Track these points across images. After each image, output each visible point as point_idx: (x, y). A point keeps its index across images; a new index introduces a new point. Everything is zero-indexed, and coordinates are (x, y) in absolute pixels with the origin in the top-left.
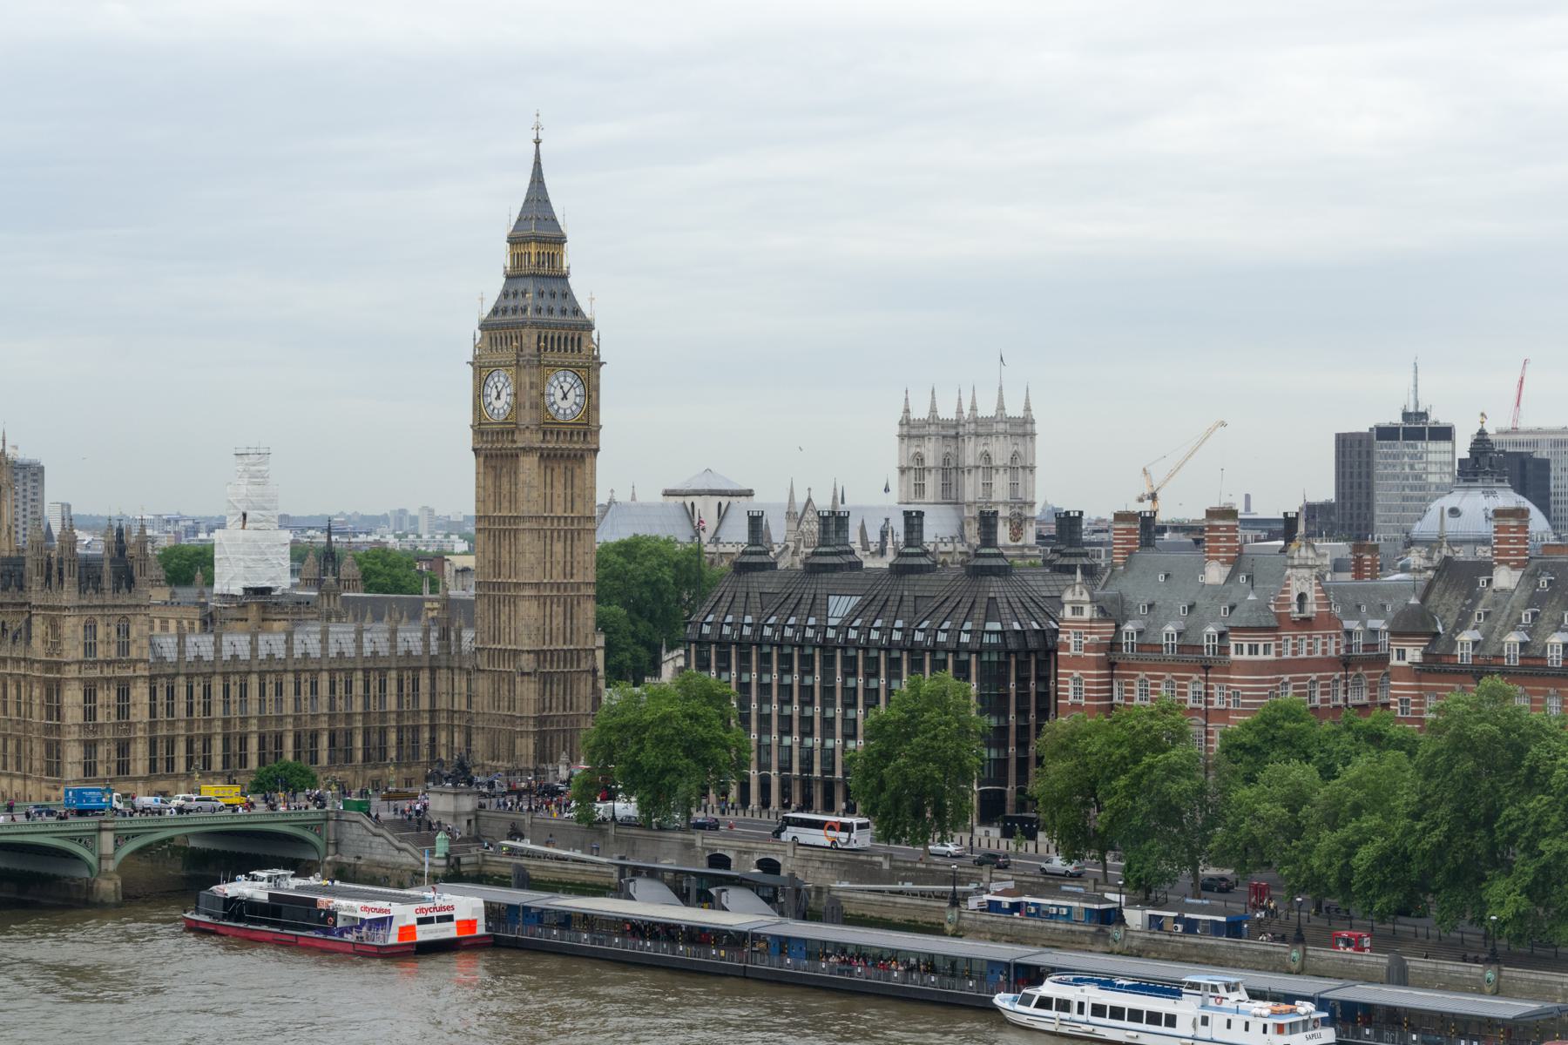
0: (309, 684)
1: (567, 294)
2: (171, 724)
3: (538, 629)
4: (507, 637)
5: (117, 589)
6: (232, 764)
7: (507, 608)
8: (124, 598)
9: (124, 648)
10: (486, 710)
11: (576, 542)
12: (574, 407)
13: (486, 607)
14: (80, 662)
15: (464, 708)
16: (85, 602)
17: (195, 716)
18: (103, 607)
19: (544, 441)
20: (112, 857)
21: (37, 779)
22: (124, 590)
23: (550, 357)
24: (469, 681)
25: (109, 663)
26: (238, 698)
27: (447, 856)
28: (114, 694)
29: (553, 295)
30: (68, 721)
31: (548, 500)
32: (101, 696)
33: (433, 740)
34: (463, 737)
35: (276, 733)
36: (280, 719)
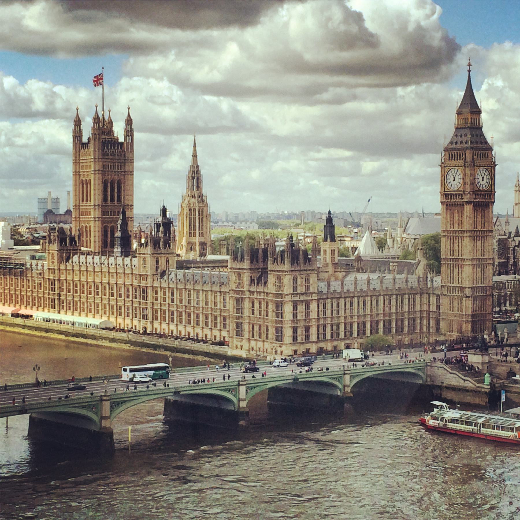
1: (482, 135)
2: (325, 319)
7: (457, 269)
9: (308, 288)
12: (486, 184)
14: (292, 294)
15: (435, 310)
16: (293, 269)
18: (300, 271)
19: (475, 199)
20: (348, 386)
25: (302, 294)
27: (491, 384)
28: (304, 307)
31: (475, 224)
32: (299, 307)
33: (420, 323)
35: (363, 322)
36: (365, 316)
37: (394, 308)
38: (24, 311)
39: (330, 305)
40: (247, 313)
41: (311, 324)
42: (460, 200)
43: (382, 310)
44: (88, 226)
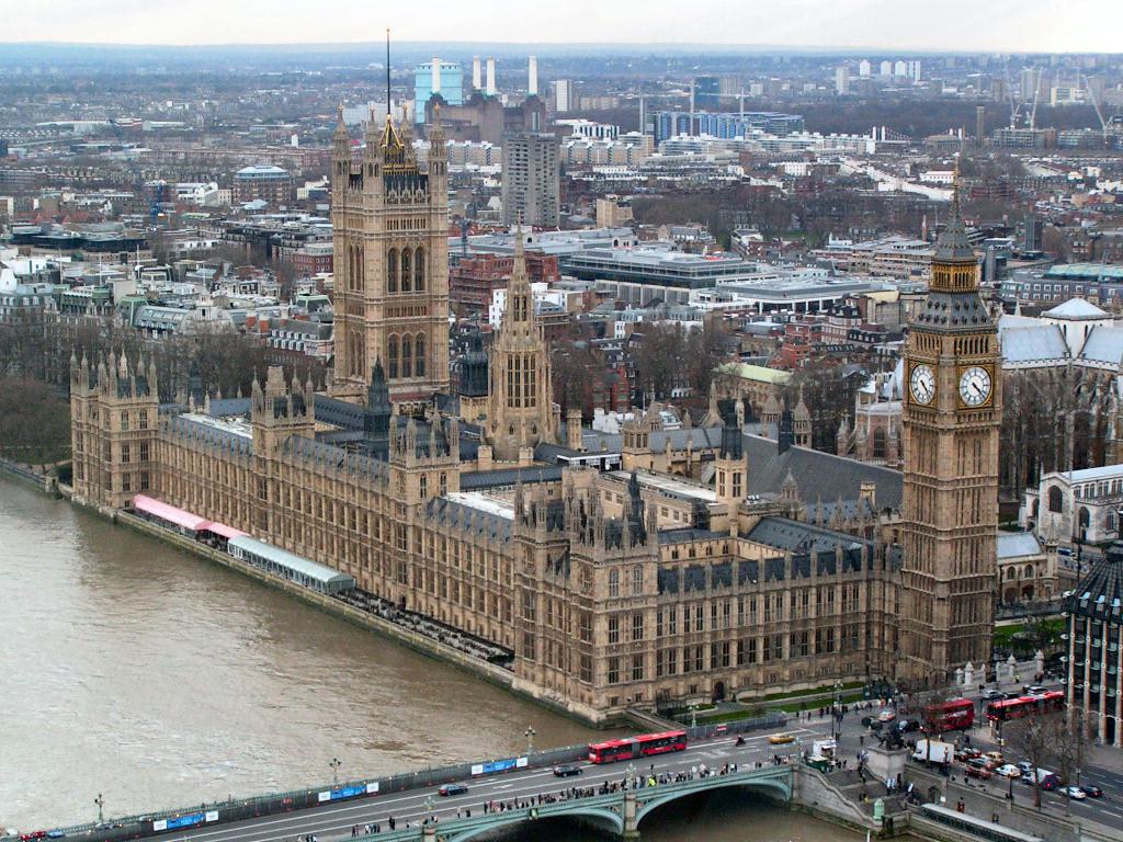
2: (673, 639)
3: (951, 565)
5: (633, 544)
8: (639, 550)
9: (638, 585)
11: (982, 495)
15: (892, 612)
16: (610, 556)
17: (691, 631)
18: (623, 559)
19: (959, 423)
22: (639, 544)
23: (964, 359)
24: (897, 598)
27: (883, 818)
28: (631, 621)
29: (966, 307)
30: (598, 645)
31: (961, 467)
33: (868, 632)
34: (891, 632)
38: (219, 528)
40: (540, 622)
41: (644, 651)
42: (932, 425)
43: (788, 615)
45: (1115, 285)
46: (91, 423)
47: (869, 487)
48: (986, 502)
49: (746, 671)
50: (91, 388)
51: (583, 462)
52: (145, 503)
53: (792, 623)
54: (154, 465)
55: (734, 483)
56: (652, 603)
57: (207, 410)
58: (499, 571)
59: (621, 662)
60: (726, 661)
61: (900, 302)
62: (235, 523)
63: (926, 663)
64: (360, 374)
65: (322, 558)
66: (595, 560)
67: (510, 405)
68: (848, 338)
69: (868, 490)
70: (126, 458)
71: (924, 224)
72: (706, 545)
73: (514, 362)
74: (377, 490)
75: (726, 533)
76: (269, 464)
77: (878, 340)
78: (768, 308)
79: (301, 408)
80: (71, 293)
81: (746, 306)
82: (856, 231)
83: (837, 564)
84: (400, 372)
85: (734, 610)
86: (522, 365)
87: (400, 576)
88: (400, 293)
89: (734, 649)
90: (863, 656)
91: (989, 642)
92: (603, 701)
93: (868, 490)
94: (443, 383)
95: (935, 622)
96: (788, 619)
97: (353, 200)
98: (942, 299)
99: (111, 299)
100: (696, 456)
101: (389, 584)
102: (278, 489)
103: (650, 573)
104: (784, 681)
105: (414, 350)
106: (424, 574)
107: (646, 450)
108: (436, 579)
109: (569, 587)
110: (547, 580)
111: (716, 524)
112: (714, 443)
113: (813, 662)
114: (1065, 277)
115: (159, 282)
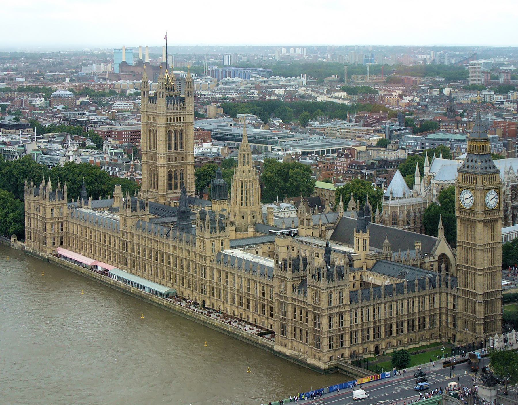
0: (400, 304)
2: (356, 326)
4: (471, 286)
6: (376, 337)
8: (341, 283)
9: (341, 301)
10: (462, 311)
13: (462, 274)
15: (452, 308)
16: (329, 286)
17: (364, 322)
18: (334, 287)
21: (310, 347)
25: (336, 307)
26: (378, 313)
28: (338, 318)
30: (324, 330)
33: (440, 318)
36: (391, 318)
37: (417, 308)
39: (360, 313)
40: (290, 317)
44: (155, 170)
45: (457, 143)
46: (35, 213)
47: (419, 244)
48: (497, 255)
49: (388, 340)
50: (35, 196)
51: (282, 233)
52: (62, 251)
53: (408, 315)
54: (65, 233)
55: (364, 244)
56: (347, 308)
57: (89, 207)
58: (258, 290)
59: (334, 338)
60: (380, 335)
61: (367, 151)
62: (109, 262)
63: (472, 333)
64: (154, 188)
65: (158, 281)
66: (322, 288)
67: (242, 205)
68: (348, 168)
69: (418, 245)
70: (53, 230)
71: (348, 115)
72: (353, 275)
73: (243, 185)
74: (189, 248)
75: (361, 269)
76: (129, 234)
77: (362, 168)
78: (304, 154)
79: (143, 207)
80: (7, 149)
81: (297, 153)
82: (320, 119)
83: (426, 286)
84: (173, 187)
85: (383, 310)
86: (248, 186)
87: (202, 291)
88: (173, 151)
89: (383, 329)
90: (438, 330)
91: (500, 323)
92: (326, 359)
93: (418, 245)
94: (192, 192)
95: (477, 314)
96: (406, 314)
97: (151, 108)
98: (475, 158)
99: (26, 152)
100: (324, 228)
101: (195, 294)
102: (133, 245)
103: (346, 294)
104: (405, 344)
105: (179, 177)
106: (215, 290)
107: (310, 227)
108: (222, 293)
109: (305, 301)
110: (293, 297)
111: (356, 264)
112: (330, 222)
113: (417, 334)
114: (434, 139)
115: (45, 144)
